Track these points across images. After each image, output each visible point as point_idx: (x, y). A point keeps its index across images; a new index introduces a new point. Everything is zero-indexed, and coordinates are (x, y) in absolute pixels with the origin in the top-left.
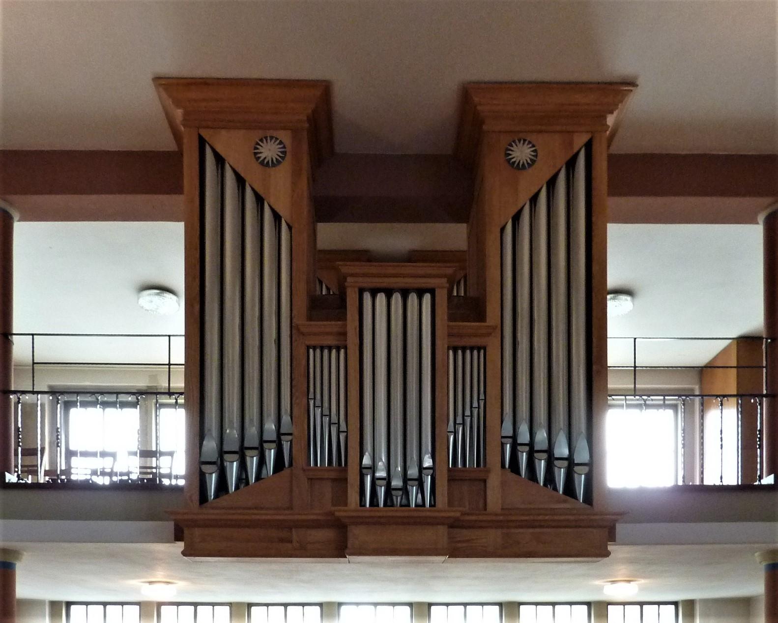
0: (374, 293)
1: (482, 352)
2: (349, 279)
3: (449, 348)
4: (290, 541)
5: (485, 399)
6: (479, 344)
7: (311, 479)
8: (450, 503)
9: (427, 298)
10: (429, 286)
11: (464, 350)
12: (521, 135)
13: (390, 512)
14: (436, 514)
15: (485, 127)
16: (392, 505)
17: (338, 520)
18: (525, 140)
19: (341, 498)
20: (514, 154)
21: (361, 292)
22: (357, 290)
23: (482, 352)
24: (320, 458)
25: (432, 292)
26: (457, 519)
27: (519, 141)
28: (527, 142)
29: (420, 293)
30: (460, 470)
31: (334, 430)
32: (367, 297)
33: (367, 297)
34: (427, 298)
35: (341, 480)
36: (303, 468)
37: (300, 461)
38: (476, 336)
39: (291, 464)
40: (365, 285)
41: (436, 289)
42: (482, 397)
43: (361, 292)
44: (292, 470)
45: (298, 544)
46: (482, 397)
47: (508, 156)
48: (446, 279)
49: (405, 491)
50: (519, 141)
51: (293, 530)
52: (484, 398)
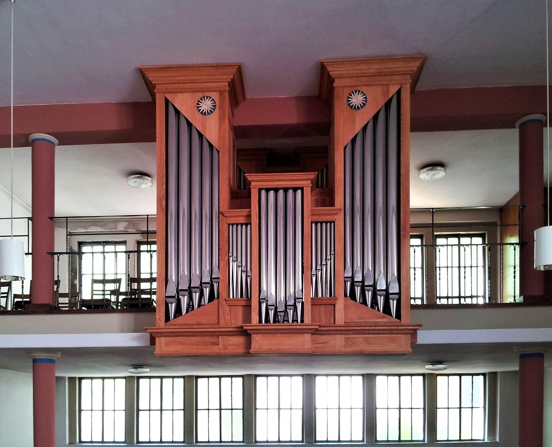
0: (268, 190)
1: (333, 224)
2: (253, 183)
3: (312, 223)
4: (218, 344)
5: (334, 254)
6: (330, 220)
7: (230, 306)
8: (313, 320)
9: (299, 192)
10: (300, 186)
11: (322, 223)
12: (358, 88)
13: (277, 326)
14: (304, 327)
15: (334, 85)
16: (279, 322)
17: (246, 331)
18: (359, 91)
19: (247, 318)
20: (352, 100)
21: (260, 190)
22: (257, 190)
23: (333, 224)
24: (234, 293)
25: (302, 189)
26: (317, 329)
27: (356, 92)
28: (360, 93)
29: (295, 190)
30: (320, 299)
31: (244, 275)
32: (263, 193)
33: (263, 193)
34: (299, 192)
35: (248, 307)
36: (225, 299)
37: (223, 295)
38: (328, 215)
39: (218, 297)
40: (261, 187)
41: (304, 188)
42: (332, 253)
43: (260, 190)
44: (219, 301)
45: (223, 347)
46: (332, 253)
47: (349, 102)
48: (310, 181)
49: (285, 311)
50: (356, 92)
51: (220, 337)
52: (334, 253)
